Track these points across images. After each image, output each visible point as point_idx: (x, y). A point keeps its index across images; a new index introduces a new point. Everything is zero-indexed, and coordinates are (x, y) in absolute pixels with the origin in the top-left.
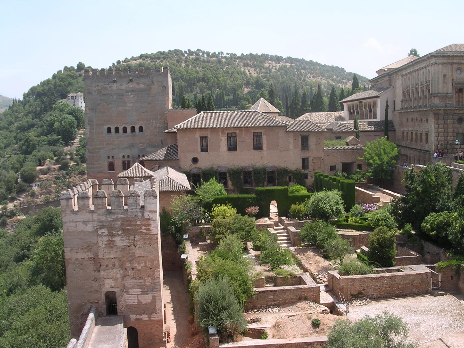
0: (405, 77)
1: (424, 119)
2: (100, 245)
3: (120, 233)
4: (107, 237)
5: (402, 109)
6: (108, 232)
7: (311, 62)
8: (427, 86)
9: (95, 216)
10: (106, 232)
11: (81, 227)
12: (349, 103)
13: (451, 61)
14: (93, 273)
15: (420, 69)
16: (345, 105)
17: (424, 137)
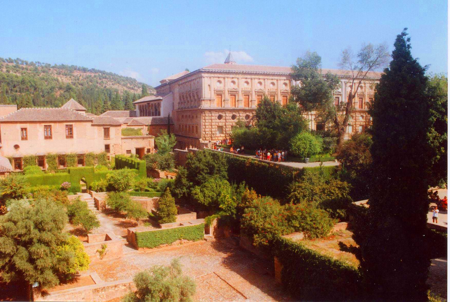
1: (195, 116)
5: (179, 109)
8: (196, 92)
12: (139, 104)
16: (137, 106)
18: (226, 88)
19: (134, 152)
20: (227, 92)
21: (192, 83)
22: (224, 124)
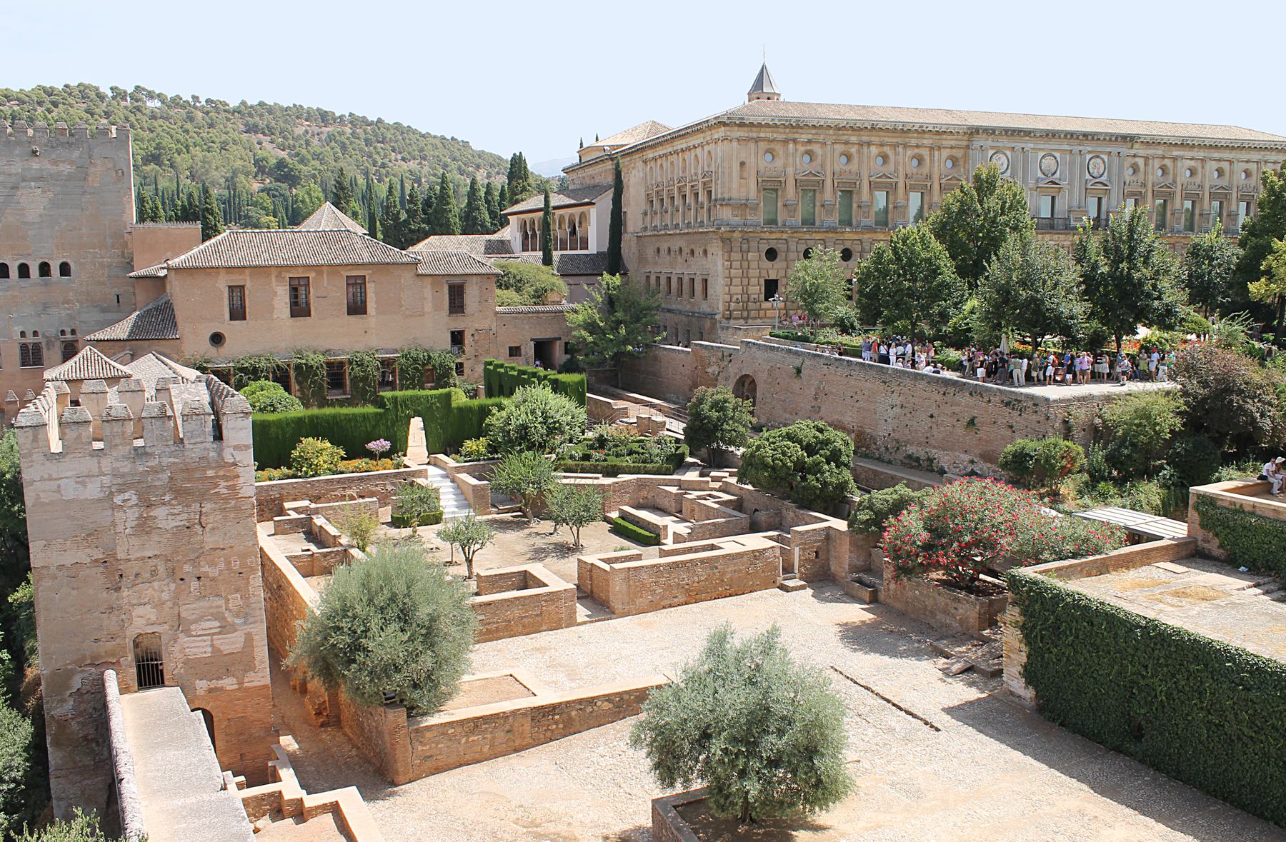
0: (653, 163)
1: (699, 251)
2: (120, 528)
3: (167, 498)
4: (136, 509)
6: (139, 499)
7: (397, 126)
9: (106, 464)
10: (134, 497)
11: (70, 491)
13: (755, 135)
14: (105, 594)
15: (689, 149)
17: (698, 287)
18: (790, 171)
19: (529, 350)
20: (791, 182)
21: (690, 156)
22: (782, 273)
